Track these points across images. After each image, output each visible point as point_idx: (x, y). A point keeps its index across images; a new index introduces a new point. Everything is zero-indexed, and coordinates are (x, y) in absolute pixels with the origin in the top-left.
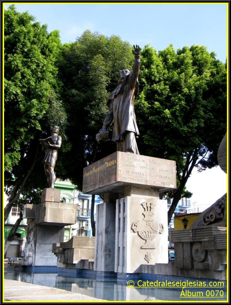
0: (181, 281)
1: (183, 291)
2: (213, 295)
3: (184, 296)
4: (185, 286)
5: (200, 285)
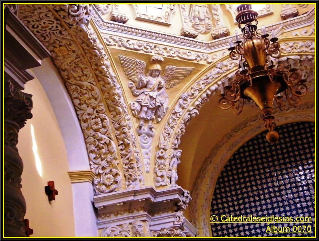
1: (268, 226)
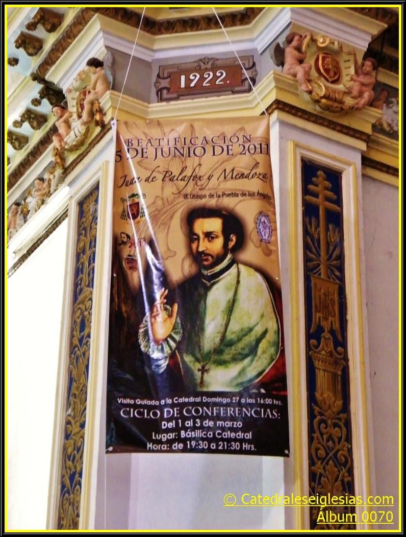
0: (318, 494)
2: (373, 518)
3: (324, 521)
4: (325, 503)
5: (352, 502)
